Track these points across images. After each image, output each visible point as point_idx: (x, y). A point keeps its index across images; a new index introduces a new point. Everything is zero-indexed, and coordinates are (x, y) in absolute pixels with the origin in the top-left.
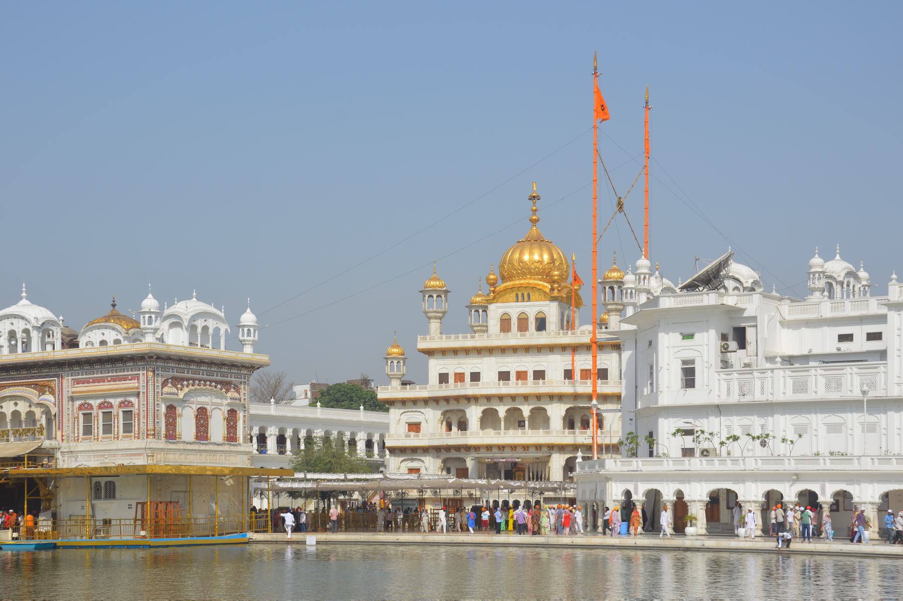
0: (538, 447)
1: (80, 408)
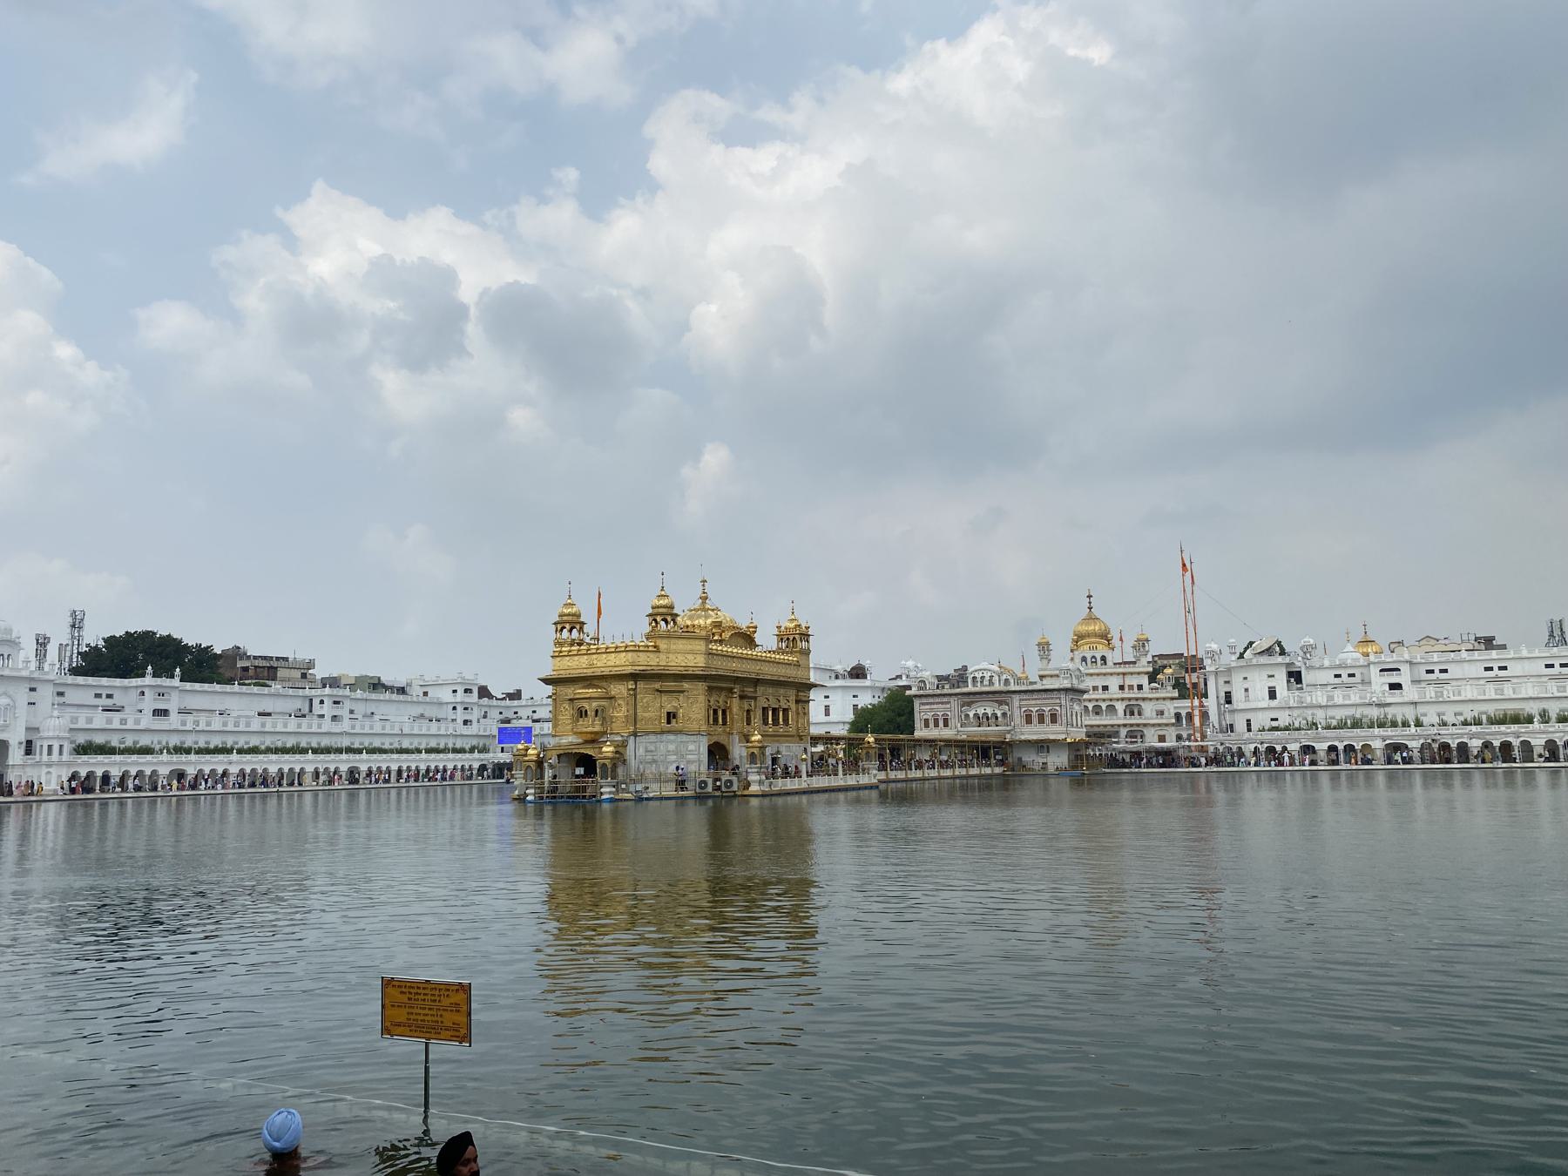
0: (1112, 726)
1: (1025, 711)
